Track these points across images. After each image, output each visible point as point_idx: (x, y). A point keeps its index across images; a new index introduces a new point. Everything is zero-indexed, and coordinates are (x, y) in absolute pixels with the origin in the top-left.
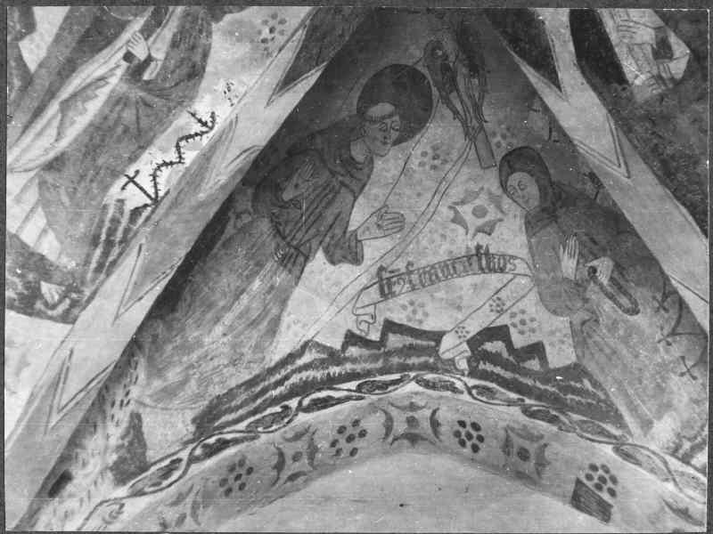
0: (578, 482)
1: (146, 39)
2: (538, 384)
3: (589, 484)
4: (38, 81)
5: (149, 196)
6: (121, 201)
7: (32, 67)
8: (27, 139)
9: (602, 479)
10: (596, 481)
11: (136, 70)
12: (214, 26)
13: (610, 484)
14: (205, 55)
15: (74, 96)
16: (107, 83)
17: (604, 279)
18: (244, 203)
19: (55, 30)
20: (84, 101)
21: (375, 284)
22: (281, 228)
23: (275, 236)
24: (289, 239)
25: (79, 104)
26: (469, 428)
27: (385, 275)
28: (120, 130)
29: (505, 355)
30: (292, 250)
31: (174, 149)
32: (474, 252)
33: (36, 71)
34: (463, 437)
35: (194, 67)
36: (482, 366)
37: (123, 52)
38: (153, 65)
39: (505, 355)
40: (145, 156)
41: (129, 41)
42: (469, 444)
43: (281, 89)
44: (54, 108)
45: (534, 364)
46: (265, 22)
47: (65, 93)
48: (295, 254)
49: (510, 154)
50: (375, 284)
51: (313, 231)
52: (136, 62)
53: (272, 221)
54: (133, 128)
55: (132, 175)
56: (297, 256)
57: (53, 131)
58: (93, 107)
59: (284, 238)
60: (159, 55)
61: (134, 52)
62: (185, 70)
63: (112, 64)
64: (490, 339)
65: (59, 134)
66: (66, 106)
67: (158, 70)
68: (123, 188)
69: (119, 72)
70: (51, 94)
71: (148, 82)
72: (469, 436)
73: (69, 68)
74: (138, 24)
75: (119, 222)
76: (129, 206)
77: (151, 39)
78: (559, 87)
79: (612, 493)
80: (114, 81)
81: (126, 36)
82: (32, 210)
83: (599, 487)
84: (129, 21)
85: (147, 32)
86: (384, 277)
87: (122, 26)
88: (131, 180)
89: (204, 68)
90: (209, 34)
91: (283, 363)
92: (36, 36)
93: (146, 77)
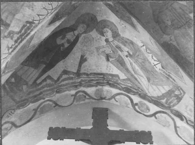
1: (123, 51)
4: (129, 78)
5: (159, 63)
6: (160, 69)
7: (126, 78)
8: (142, 84)
11: (129, 55)
12: (121, 36)
14: (128, 39)
15: (134, 70)
16: (132, 63)
18: (166, 38)
19: (119, 70)
20: (135, 69)
22: (179, 26)
23: (181, 29)
24: (183, 24)
25: (136, 70)
28: (143, 64)
31: (149, 54)
33: (127, 77)
35: (131, 43)
37: (126, 58)
38: (129, 52)
40: (150, 60)
41: (123, 55)
43: (135, 28)
44: (136, 76)
46: (121, 25)
47: (133, 73)
48: (188, 23)
51: (183, 16)
52: (128, 55)
53: (176, 29)
54: (143, 61)
55: (154, 65)
56: (189, 22)
57: (141, 78)
58: (137, 68)
59: (183, 26)
60: (127, 50)
61: (126, 55)
62: (131, 46)
63: (128, 61)
65: (142, 76)
66: (135, 73)
67: (130, 51)
68: (157, 68)
69: (130, 60)
70: (132, 75)
71: (133, 54)
73: (127, 70)
74: (120, 53)
75: (164, 72)
76: (161, 68)
77: (123, 50)
80: (132, 61)
81: (122, 56)
82: (158, 88)
84: (119, 54)
85: (122, 51)
87: (120, 56)
88: (155, 65)
89: (131, 41)
90: (123, 37)
92: (119, 75)
93: (131, 54)
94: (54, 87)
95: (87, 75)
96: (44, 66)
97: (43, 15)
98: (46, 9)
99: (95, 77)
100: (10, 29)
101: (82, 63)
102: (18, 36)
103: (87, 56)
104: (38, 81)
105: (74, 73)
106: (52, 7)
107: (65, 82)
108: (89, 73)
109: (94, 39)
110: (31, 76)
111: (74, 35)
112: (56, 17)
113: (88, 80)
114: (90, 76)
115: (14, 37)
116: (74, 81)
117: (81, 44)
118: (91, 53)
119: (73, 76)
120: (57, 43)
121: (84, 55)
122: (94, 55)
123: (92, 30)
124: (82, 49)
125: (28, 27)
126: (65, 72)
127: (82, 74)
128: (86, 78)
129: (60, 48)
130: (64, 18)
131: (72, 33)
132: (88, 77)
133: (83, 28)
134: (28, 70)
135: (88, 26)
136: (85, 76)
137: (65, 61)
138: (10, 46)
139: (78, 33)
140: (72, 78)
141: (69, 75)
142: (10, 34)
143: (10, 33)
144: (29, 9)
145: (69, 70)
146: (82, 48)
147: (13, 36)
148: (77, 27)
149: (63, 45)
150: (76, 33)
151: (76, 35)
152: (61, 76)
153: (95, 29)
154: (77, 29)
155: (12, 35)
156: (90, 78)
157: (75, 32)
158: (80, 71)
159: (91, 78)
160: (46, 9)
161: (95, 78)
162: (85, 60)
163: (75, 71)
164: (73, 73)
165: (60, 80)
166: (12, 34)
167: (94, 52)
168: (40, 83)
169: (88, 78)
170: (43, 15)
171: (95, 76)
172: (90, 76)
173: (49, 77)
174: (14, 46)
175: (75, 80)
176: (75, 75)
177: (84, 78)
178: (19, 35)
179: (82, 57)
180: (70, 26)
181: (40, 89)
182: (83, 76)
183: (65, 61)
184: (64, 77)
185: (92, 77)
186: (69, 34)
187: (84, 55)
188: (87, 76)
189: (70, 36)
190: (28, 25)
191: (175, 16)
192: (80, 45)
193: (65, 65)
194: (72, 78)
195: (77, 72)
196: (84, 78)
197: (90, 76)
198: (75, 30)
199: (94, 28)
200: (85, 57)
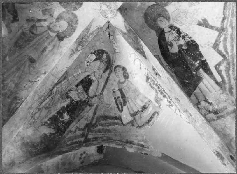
94: (231, 62)
95: (224, 19)
96: (201, 70)
97: (140, 64)
98: (135, 60)
99: (229, 8)
100: (153, 100)
101: (208, 24)
102: (159, 93)
103: (200, 19)
104: (219, 80)
105: (219, 36)
106: (132, 54)
107: (228, 48)
108: (223, 16)
109: (178, 8)
110: (209, 87)
111: (170, 32)
112: (139, 51)
113: (231, 17)
114: (227, 14)
115: (160, 98)
116: (229, 37)
117: (183, 25)
118: (196, 12)
119: (223, 36)
120: (176, 53)
121: (198, 21)
122: (199, 9)
123: (166, 11)
124: (189, 24)
125: (151, 81)
126: (215, 46)
127: (222, 26)
128: (228, 20)
129: (183, 49)
130: (141, 42)
131: (167, 35)
132: (227, 17)
133: (162, 22)
134: (200, 89)
135: (160, 15)
136: (226, 21)
137: (201, 45)
138: (169, 103)
139: (168, 28)
140: (225, 39)
141: (220, 42)
142: (158, 101)
143: (157, 101)
144: (135, 78)
145: (213, 41)
146: (188, 24)
147: (159, 98)
148: (160, 28)
149: (180, 46)
150: (167, 29)
151: (170, 30)
152: (220, 53)
153: (165, 7)
154: (163, 28)
155: (158, 100)
156: (229, 15)
157: (166, 30)
158: (218, 28)
159: (230, 14)
160: (135, 60)
161: (230, 8)
162: (205, 20)
163: (217, 33)
164: (218, 36)
165: (225, 53)
166: (157, 99)
167: (195, 10)
168: (222, 78)
169: (228, 17)
170: (140, 64)
171: (228, 8)
172: (227, 14)
173: (217, 67)
174: (169, 99)
175: (228, 34)
176: (222, 34)
177: (227, 23)
178: (158, 92)
179: (200, 24)
180: (157, 36)
181: (230, 79)
182: (225, 23)
183: (201, 45)
184: (221, 47)
185: (229, 13)
186: (167, 38)
187: (198, 21)
188: (226, 19)
189: (170, 37)
190: (150, 81)
192: (184, 26)
193: (209, 47)
194: (225, 39)
195: (218, 31)
196: (227, 23)
197: (226, 14)
198: (163, 30)
199: (164, 8)
200: (201, 21)
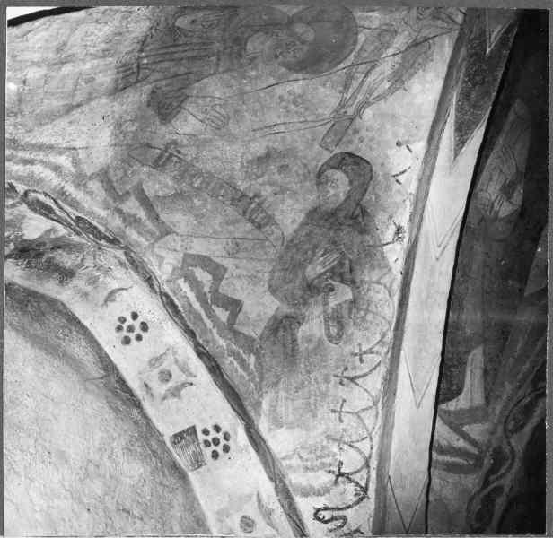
0: (193, 429)
2: (215, 331)
3: (201, 437)
9: (216, 442)
10: (209, 438)
13: (219, 449)
17: (333, 303)
21: (160, 149)
26: (137, 324)
27: (172, 150)
29: (206, 289)
30: (135, 65)
32: (251, 195)
34: (125, 326)
36: (181, 282)
39: (206, 289)
42: (125, 333)
45: (223, 315)
49: (351, 155)
50: (160, 149)
64: (204, 267)
72: (131, 329)
78: (456, 155)
79: (215, 455)
83: (207, 444)
86: (169, 151)
91: (41, 147)
191: (180, 48)
